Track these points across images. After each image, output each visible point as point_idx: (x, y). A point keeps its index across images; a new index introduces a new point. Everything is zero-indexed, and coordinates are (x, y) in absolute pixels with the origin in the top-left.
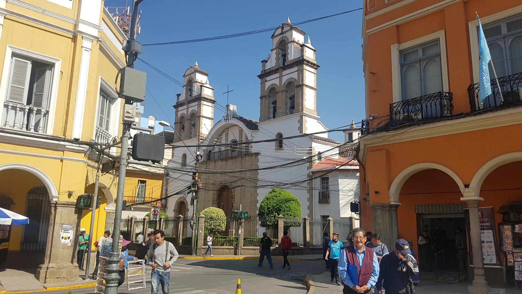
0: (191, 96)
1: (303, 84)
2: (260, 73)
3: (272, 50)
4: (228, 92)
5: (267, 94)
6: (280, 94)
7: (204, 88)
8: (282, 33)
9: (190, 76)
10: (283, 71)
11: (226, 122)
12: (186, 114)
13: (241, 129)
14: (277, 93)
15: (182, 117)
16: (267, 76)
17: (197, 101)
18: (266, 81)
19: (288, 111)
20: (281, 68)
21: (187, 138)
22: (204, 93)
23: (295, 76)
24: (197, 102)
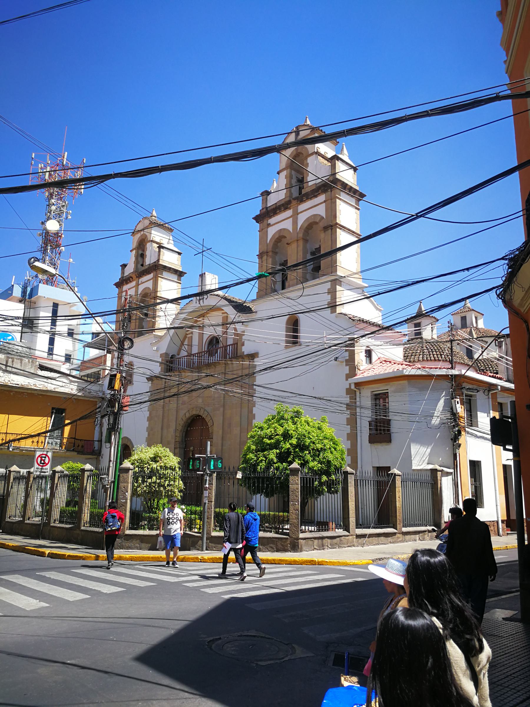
0: (142, 265)
1: (337, 224)
2: (258, 213)
3: (278, 173)
5: (270, 248)
6: (294, 246)
9: (142, 233)
10: (300, 205)
11: (199, 303)
14: (288, 244)
16: (270, 217)
17: (152, 272)
18: (269, 225)
19: (308, 276)
20: (296, 199)
21: (134, 336)
23: (321, 210)
24: (152, 274)
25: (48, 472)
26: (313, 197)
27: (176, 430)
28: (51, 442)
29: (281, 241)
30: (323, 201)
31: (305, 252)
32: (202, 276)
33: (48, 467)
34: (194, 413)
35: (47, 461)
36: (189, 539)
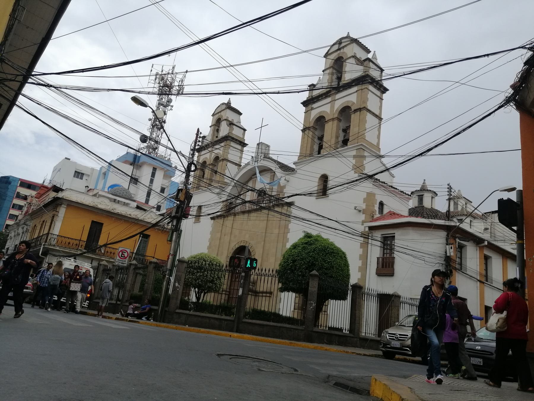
0: (217, 137)
2: (305, 99)
4: (261, 127)
6: (330, 123)
7: (234, 127)
8: (339, 49)
9: (220, 114)
10: (337, 93)
12: (208, 158)
13: (273, 174)
14: (326, 122)
15: (205, 162)
16: (314, 103)
18: (312, 109)
20: (334, 88)
22: (233, 133)
25: (126, 263)
26: (348, 88)
27: (227, 256)
28: (136, 258)
29: (321, 120)
30: (355, 91)
31: (338, 127)
32: (259, 144)
33: (127, 260)
34: (242, 244)
35: (126, 255)
36: (224, 322)
